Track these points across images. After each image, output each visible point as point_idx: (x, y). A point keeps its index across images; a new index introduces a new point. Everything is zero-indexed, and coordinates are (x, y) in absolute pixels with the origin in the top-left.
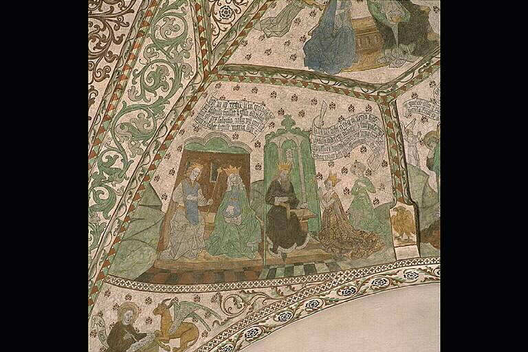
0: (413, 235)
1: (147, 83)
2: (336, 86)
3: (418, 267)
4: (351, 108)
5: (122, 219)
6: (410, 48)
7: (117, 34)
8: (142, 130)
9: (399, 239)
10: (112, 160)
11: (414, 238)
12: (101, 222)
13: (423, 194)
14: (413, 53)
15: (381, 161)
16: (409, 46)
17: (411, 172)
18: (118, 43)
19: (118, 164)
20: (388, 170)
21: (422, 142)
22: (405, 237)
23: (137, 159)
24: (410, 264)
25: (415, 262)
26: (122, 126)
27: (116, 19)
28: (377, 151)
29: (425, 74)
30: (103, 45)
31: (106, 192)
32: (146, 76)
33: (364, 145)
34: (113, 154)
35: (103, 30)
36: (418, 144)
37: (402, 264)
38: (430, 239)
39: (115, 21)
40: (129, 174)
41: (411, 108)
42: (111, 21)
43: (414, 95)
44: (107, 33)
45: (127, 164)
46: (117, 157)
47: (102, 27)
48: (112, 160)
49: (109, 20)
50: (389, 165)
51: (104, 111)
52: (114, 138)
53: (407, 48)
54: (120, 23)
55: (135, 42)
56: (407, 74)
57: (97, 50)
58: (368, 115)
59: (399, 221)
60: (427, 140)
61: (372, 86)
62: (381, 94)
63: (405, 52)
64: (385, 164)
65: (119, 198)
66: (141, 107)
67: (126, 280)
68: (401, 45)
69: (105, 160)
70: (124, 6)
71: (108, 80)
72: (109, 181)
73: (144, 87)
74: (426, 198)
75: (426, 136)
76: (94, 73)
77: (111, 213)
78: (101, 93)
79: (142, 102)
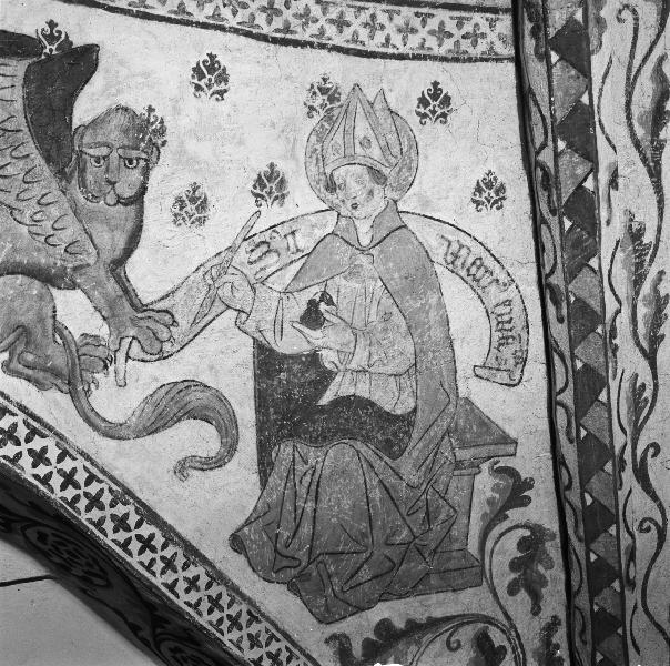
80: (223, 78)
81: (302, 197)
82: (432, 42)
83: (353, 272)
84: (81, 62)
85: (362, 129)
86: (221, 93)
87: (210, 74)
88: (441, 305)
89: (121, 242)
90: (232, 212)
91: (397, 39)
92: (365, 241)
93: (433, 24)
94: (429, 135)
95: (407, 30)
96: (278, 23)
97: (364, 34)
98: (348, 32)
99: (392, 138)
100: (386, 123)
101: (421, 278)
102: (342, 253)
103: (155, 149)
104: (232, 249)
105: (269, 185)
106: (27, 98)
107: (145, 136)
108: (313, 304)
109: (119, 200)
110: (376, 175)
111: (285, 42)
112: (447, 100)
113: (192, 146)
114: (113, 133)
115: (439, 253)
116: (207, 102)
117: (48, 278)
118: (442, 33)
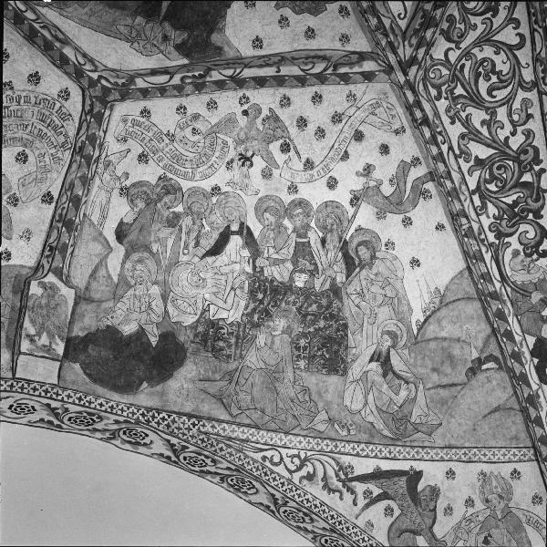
0: (58, 341)
2: (37, 26)
3: (46, 401)
4: (35, 78)
6: (178, 36)
9: (32, 341)
11: (60, 348)
13: (91, 276)
14: (178, 48)
15: (44, 191)
16: (177, 32)
17: (87, 232)
20: (49, 210)
21: (124, 191)
22: (44, 340)
24: (37, 393)
25: (46, 392)
28: (46, 170)
29: (189, 88)
33: (27, 151)
36: (116, 192)
37: (22, 388)
38: (82, 357)
41: (131, 129)
43: (145, 113)
50: (53, 205)
53: (172, 34)
56: (154, 72)
58: (58, 105)
59: (41, 307)
60: (133, 191)
61: (91, 61)
62: (104, 82)
63: (166, 38)
64: (47, 198)
68: (166, 24)
74: (94, 285)
75: (134, 185)
80: (454, 473)
81: (479, 505)
82: (512, 457)
83: (497, 527)
84: (419, 475)
85: (494, 483)
86: (454, 478)
87: (450, 474)
88: (527, 537)
89: (431, 521)
90: (460, 511)
91: (502, 458)
92: (500, 517)
93: (512, 453)
94: (514, 483)
95: (504, 455)
96: (467, 457)
97: (492, 457)
98: (487, 457)
99: (504, 485)
100: (500, 480)
101: (518, 528)
102: (493, 522)
103: (438, 495)
104: (461, 522)
105: (469, 502)
106: (407, 485)
107: (435, 492)
108: (486, 538)
109: (430, 511)
110: (501, 497)
111: (470, 462)
112: (519, 473)
113: (447, 494)
114: (427, 492)
115: (524, 520)
116: (450, 481)
117: (415, 533)
118: (515, 455)
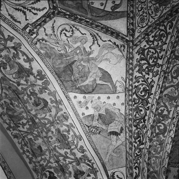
1: (174, 75)
5: (173, 136)
7: (160, 55)
8: (173, 96)
10: (162, 111)
12: (162, 140)
18: (161, 59)
19: (165, 113)
23: (173, 109)
26: (165, 96)
27: (160, 48)
30: (155, 60)
31: (162, 125)
32: (172, 72)
34: (162, 108)
35: (155, 54)
39: (159, 49)
40: (171, 116)
42: (158, 49)
44: (156, 55)
45: (169, 112)
46: (164, 109)
47: (154, 52)
48: (162, 111)
49: (157, 49)
51: (160, 89)
52: (162, 101)
54: (162, 50)
55: (170, 56)
57: (153, 63)
65: (168, 127)
66: (172, 86)
67: (175, 164)
69: (160, 112)
70: (163, 42)
71: (158, 76)
72: (163, 121)
73: (172, 77)
76: (153, 74)
77: (166, 135)
78: (156, 82)
79: (172, 84)
